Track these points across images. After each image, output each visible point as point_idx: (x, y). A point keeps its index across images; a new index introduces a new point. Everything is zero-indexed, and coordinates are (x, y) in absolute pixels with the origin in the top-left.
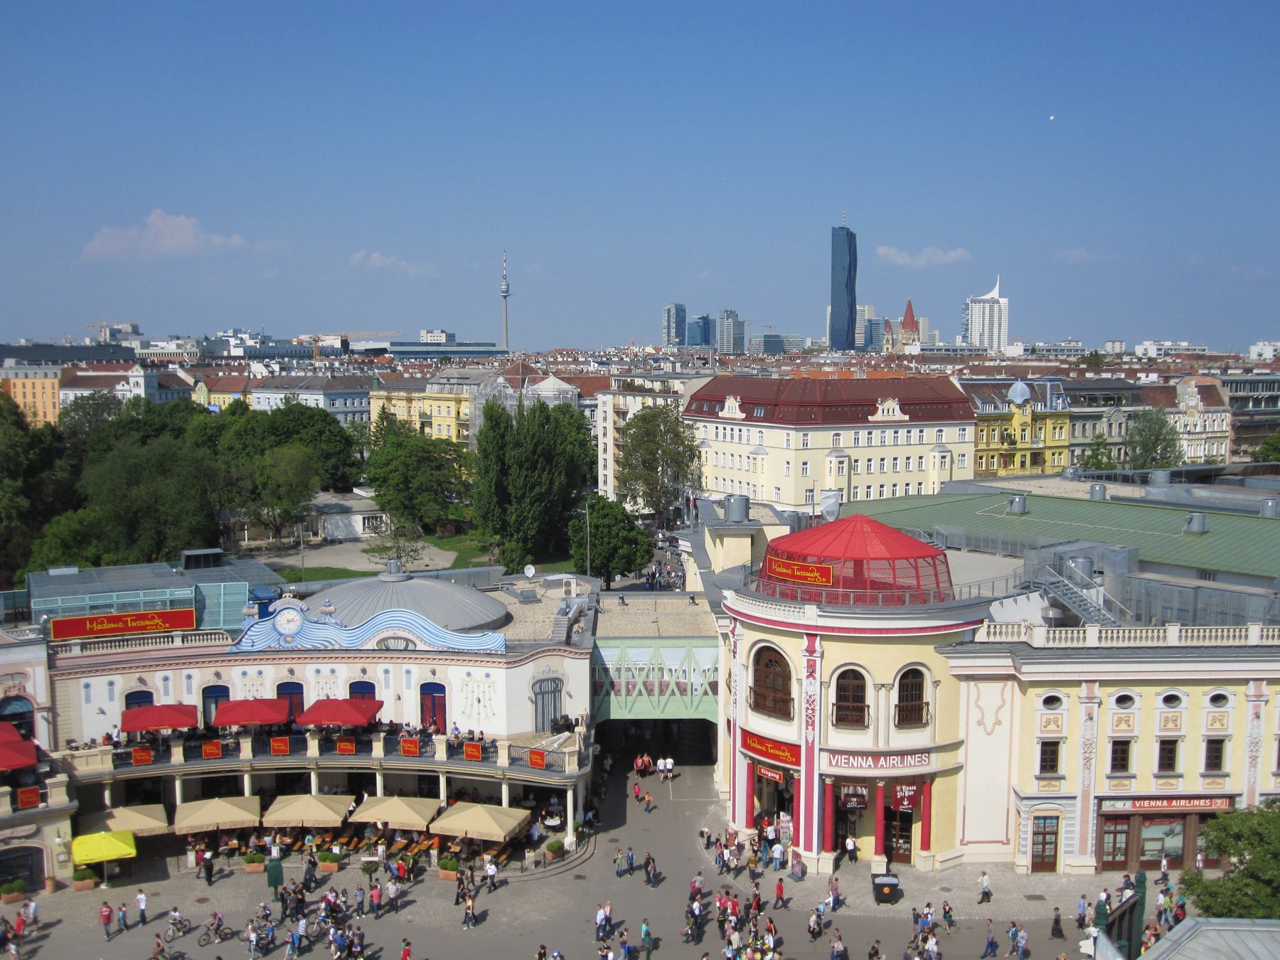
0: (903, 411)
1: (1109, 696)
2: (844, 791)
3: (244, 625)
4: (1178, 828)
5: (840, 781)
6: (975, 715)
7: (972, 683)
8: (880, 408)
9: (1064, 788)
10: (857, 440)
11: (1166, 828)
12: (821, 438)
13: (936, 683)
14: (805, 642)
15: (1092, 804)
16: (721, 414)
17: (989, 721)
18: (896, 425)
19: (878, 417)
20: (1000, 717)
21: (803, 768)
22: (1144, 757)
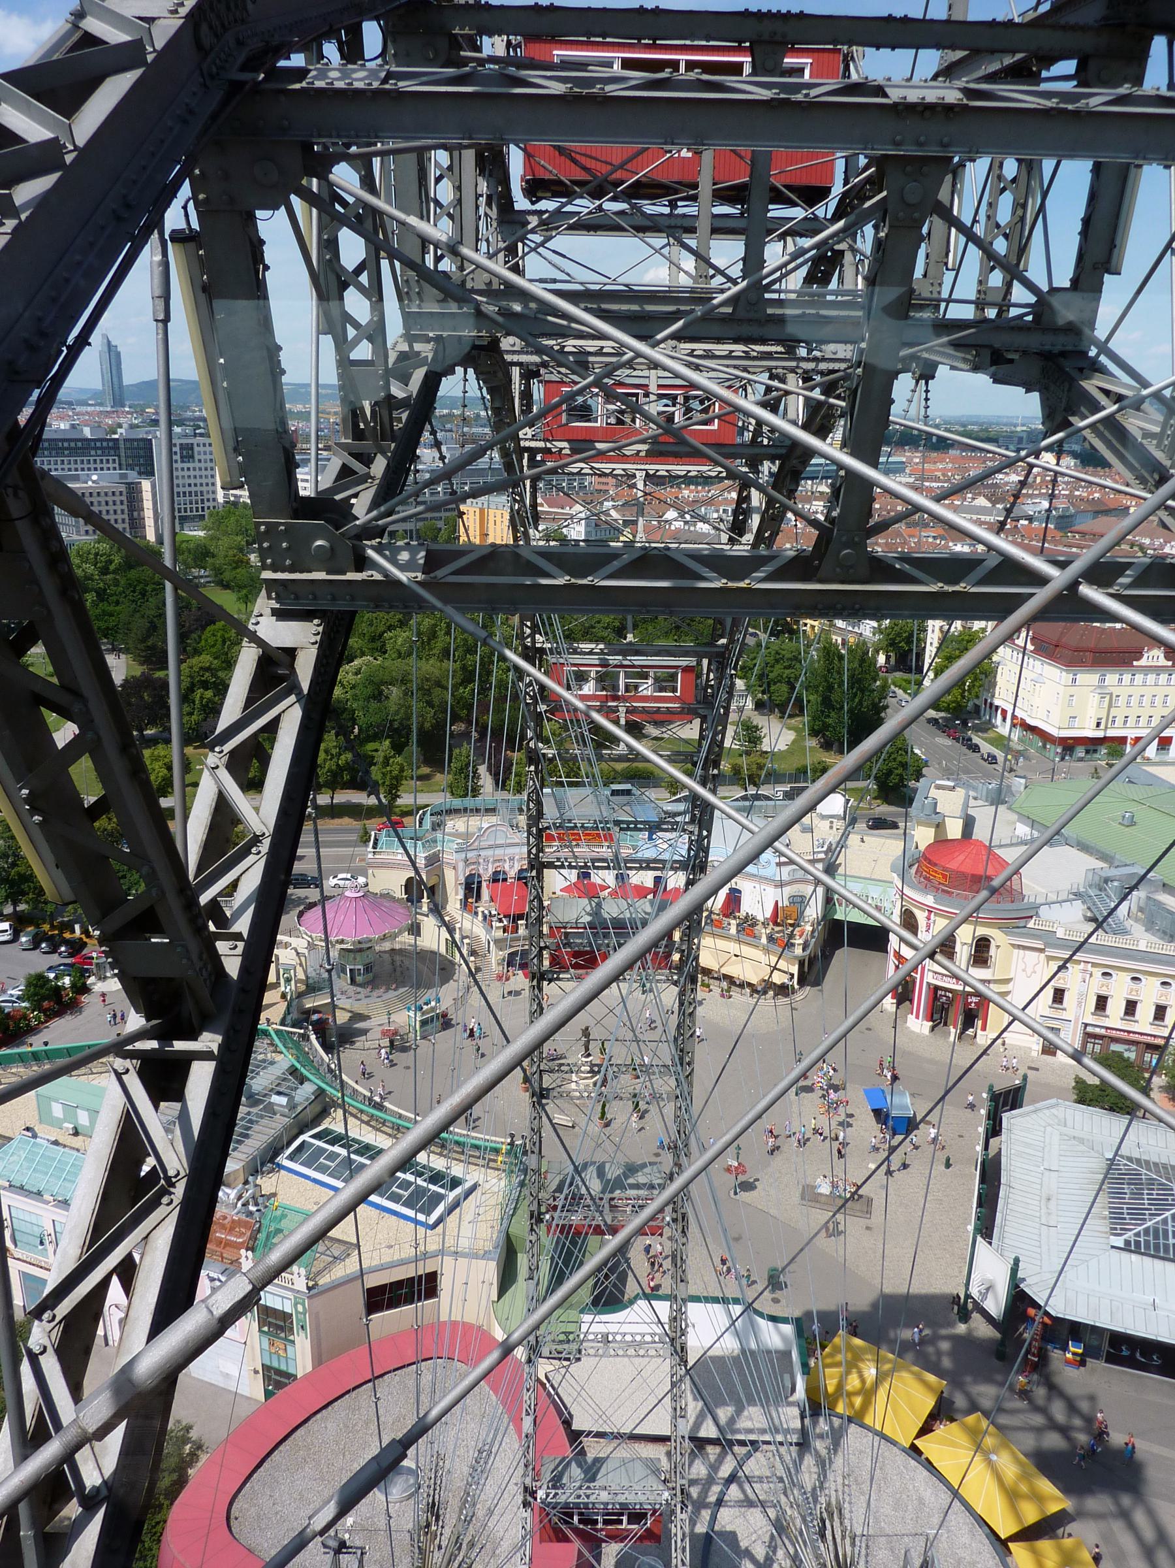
0: (1167, 658)
1: (1098, 973)
2: (940, 992)
3: (640, 844)
4: (1134, 1048)
5: (937, 988)
6: (1021, 966)
7: (1021, 952)
8: (1146, 655)
9: (1064, 1015)
10: (1120, 680)
11: (1127, 1047)
12: (1088, 678)
13: (998, 947)
14: (926, 913)
15: (1080, 1027)
16: (1017, 642)
17: (1029, 970)
18: (1158, 670)
19: (1143, 662)
20: (1036, 968)
21: (918, 976)
22: (1116, 1007)
